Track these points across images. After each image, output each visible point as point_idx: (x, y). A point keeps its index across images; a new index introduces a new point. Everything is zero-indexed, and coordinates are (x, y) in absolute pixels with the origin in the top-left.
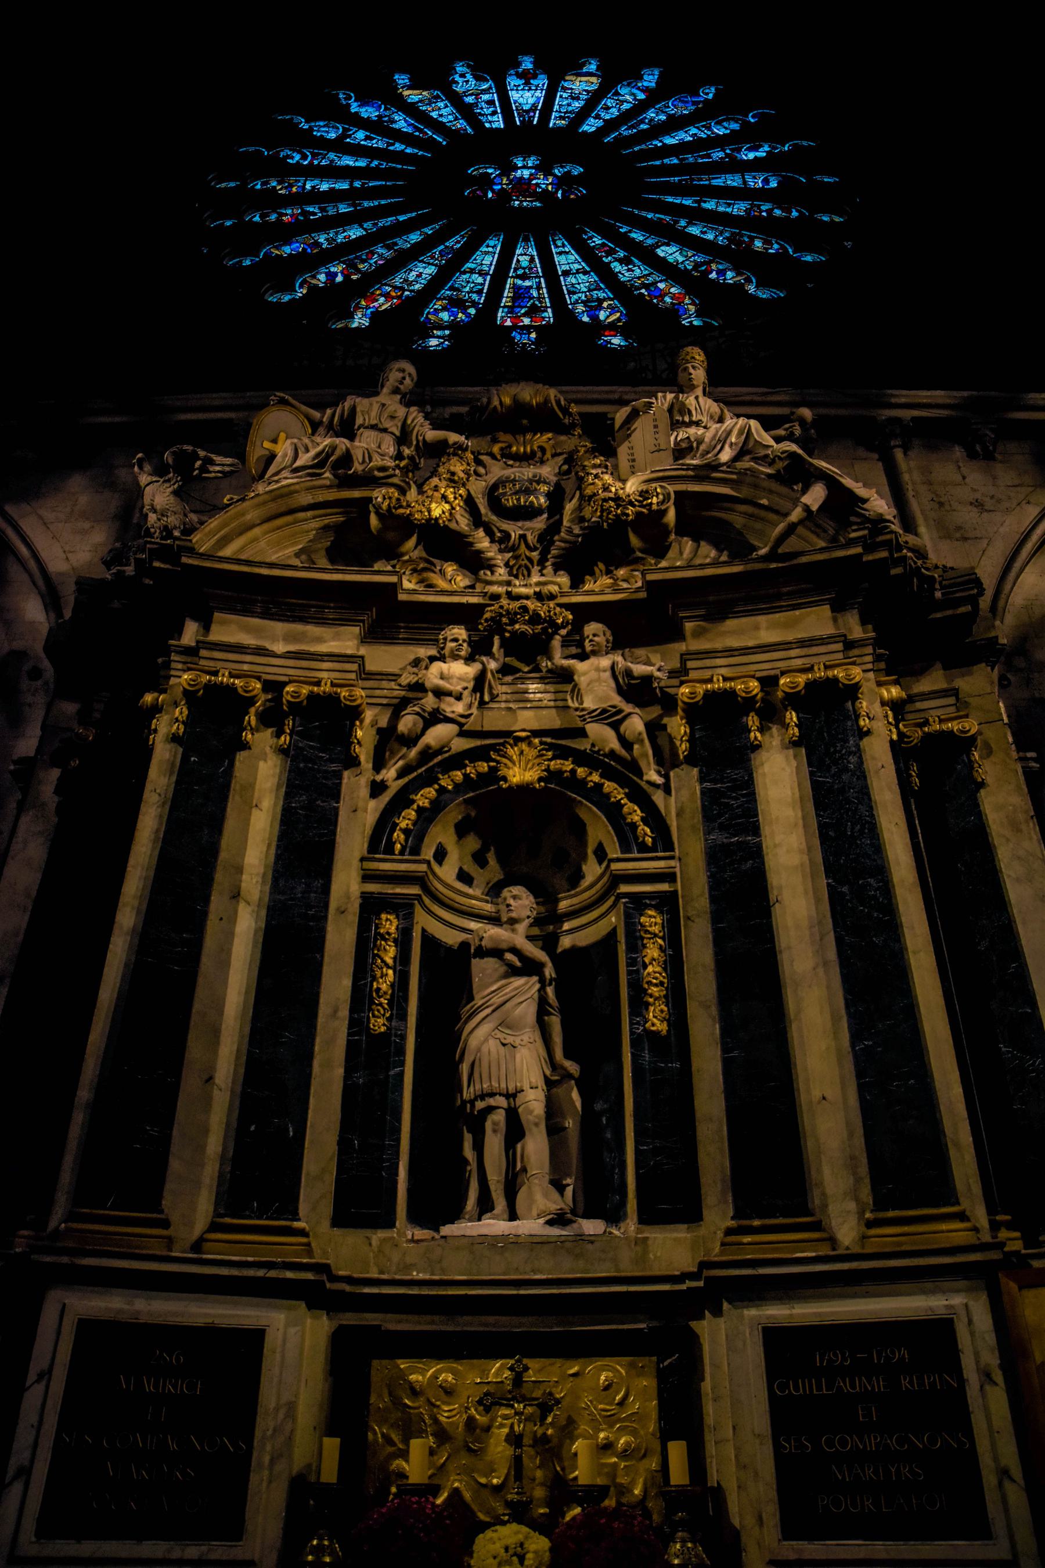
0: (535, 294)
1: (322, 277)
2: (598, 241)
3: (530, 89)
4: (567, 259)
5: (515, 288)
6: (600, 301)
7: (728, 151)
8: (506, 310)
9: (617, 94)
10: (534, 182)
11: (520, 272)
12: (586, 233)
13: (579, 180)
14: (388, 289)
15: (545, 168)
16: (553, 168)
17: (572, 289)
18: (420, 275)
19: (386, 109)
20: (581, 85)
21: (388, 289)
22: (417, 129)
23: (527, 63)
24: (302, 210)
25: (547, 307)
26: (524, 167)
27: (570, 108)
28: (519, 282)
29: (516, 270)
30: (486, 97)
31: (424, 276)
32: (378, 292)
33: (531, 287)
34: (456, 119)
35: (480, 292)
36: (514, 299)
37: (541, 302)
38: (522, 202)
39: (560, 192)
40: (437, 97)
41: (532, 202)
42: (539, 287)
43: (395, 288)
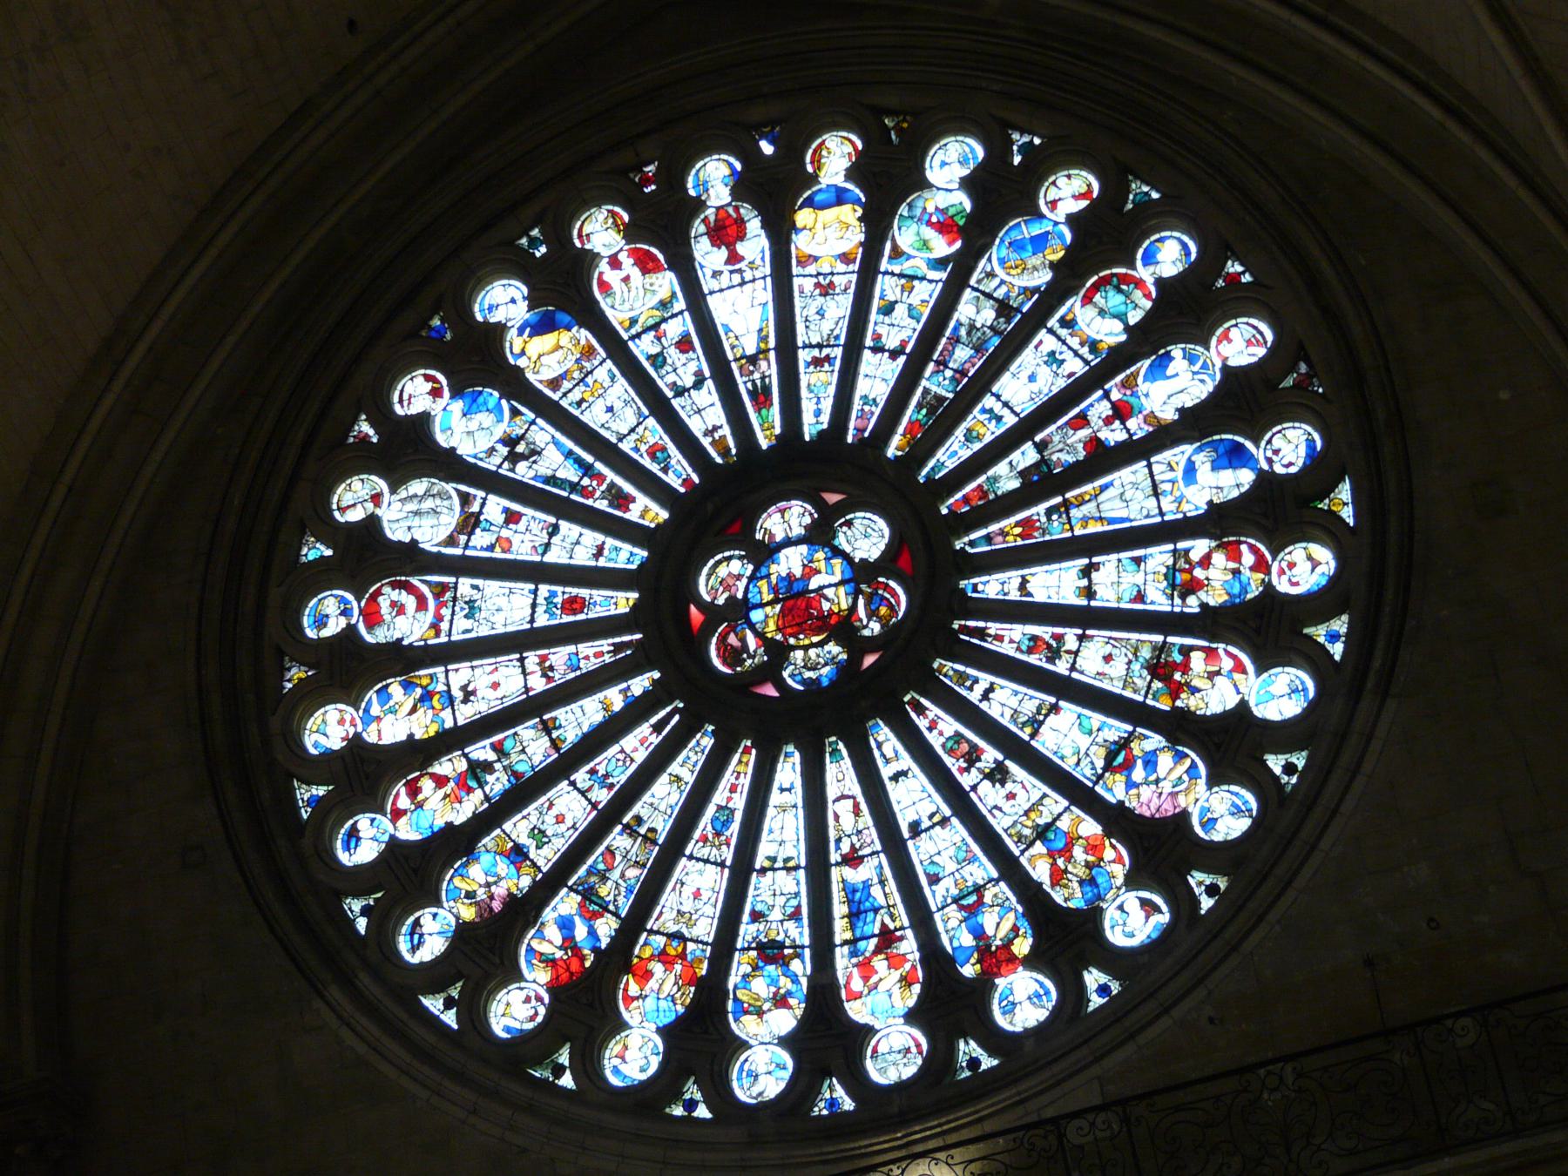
0: (881, 901)
1: (553, 933)
2: (949, 725)
3: (743, 283)
4: (913, 797)
5: (849, 890)
6: (979, 890)
7: (1115, 395)
8: (846, 949)
9: (897, 253)
10: (814, 583)
11: (845, 847)
12: (921, 711)
13: (888, 563)
14: (660, 941)
15: (820, 535)
16: (834, 537)
17: (932, 870)
18: (697, 895)
19: (515, 413)
20: (827, 233)
21: (660, 941)
22: (579, 462)
23: (714, 177)
24: (469, 760)
25: (902, 928)
26: (789, 542)
27: (826, 326)
28: (848, 872)
29: (839, 840)
30: (674, 329)
31: (705, 895)
32: (647, 953)
33: (867, 885)
34: (641, 419)
35: (795, 915)
36: (854, 916)
37: (892, 916)
38: (806, 648)
39: (861, 602)
40: (589, 352)
41: (821, 644)
42: (882, 882)
43: (672, 936)
